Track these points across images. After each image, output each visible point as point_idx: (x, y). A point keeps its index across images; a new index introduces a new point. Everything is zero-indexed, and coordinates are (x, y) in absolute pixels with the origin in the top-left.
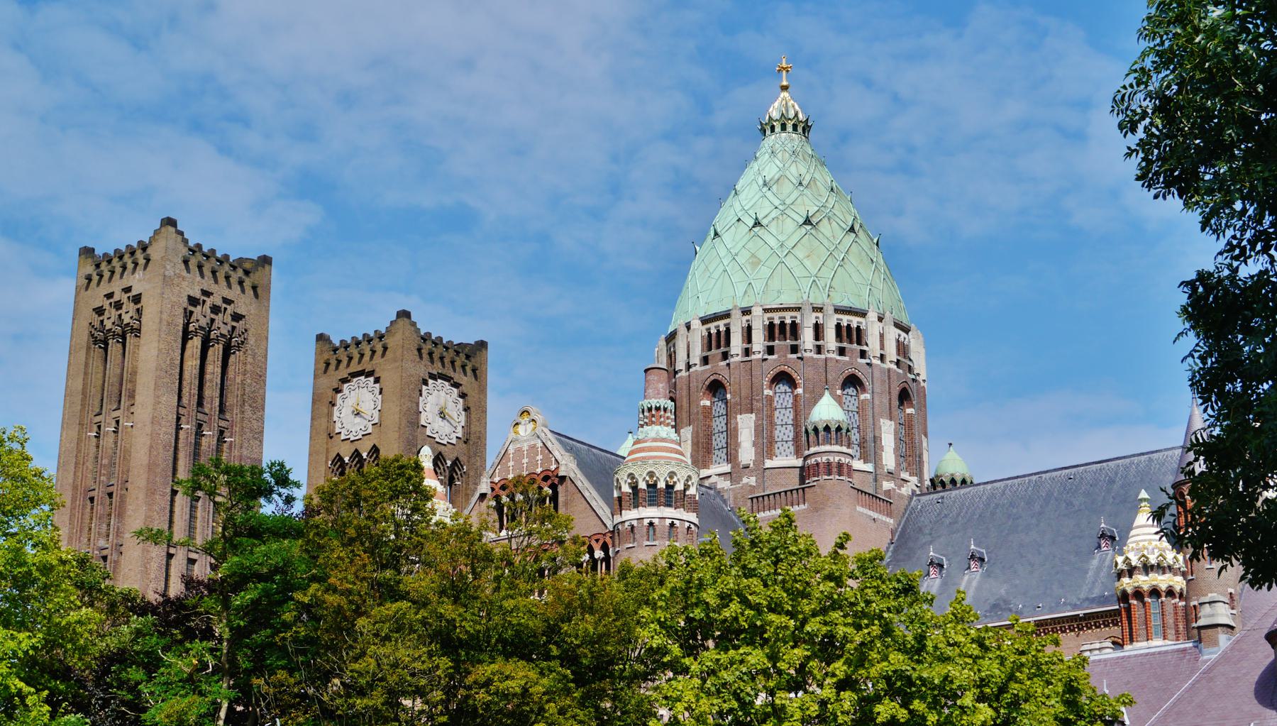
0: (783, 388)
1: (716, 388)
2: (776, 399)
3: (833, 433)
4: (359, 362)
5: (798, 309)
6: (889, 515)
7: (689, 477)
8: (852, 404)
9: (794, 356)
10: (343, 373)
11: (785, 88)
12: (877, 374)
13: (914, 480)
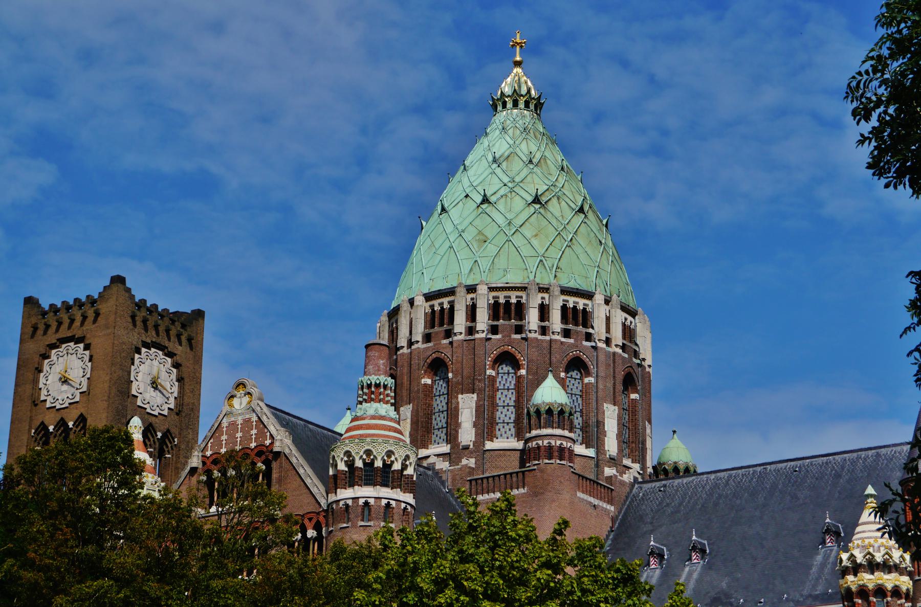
0: (506, 368)
1: (437, 366)
2: (499, 380)
3: (555, 417)
4: (69, 328)
5: (524, 289)
6: (610, 502)
7: (407, 457)
8: (576, 387)
9: (518, 336)
10: (52, 338)
11: (518, 64)
12: (602, 357)
13: (637, 467)
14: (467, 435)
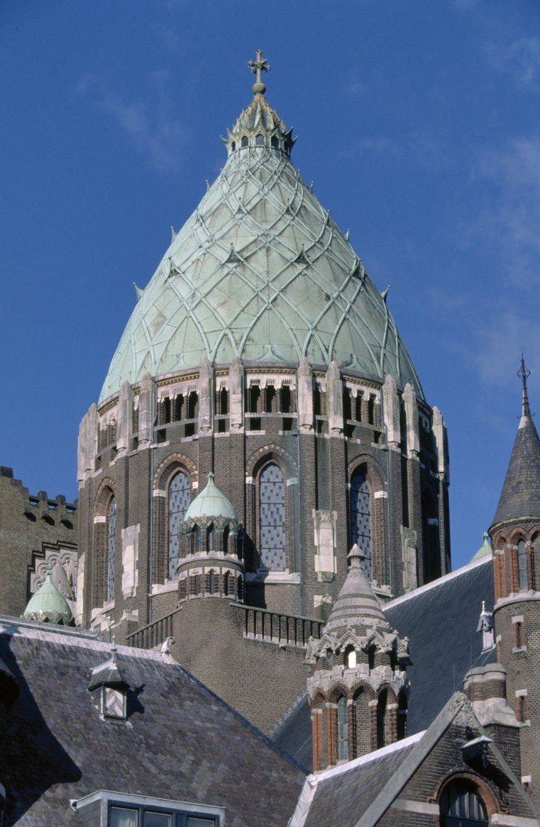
2: (171, 501)
9: (189, 439)
14: (130, 581)
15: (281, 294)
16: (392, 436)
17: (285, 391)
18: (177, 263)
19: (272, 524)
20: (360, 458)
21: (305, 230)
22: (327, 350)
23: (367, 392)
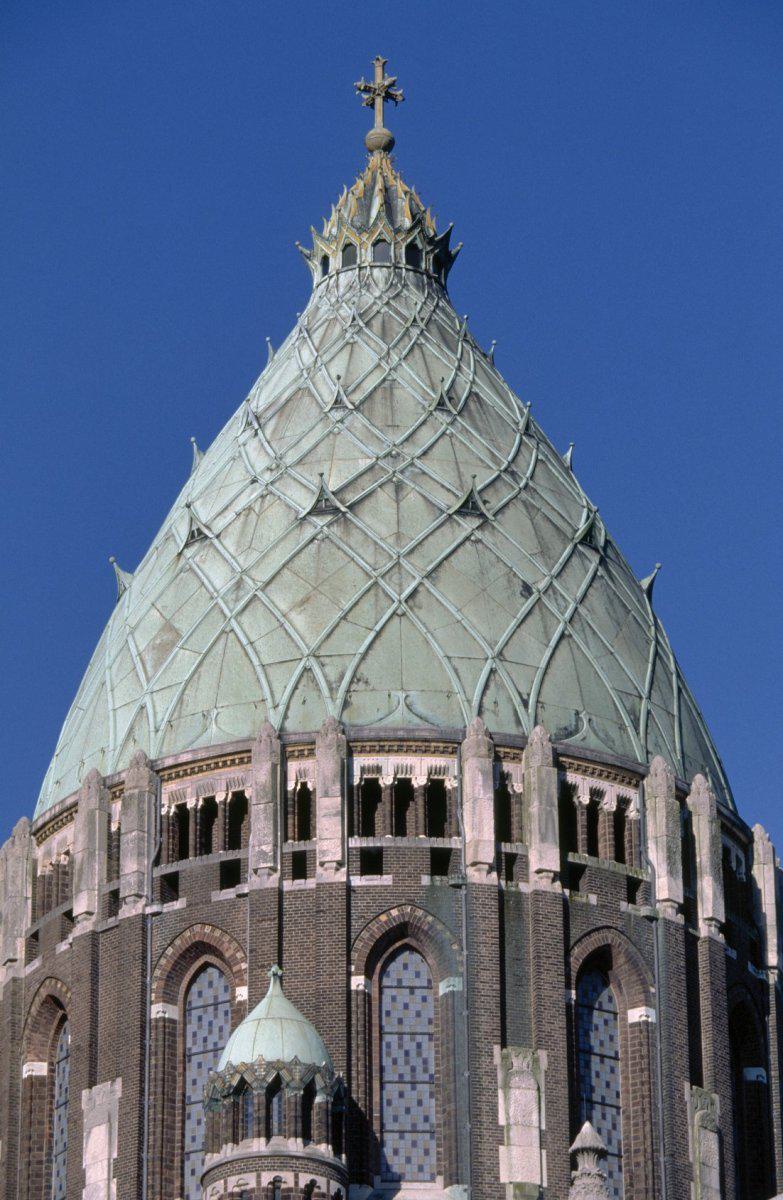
2: (191, 1028)
9: (230, 894)
15: (427, 583)
16: (666, 887)
17: (436, 792)
18: (204, 514)
19: (408, 1078)
20: (595, 936)
21: (479, 445)
22: (525, 703)
23: (612, 793)
